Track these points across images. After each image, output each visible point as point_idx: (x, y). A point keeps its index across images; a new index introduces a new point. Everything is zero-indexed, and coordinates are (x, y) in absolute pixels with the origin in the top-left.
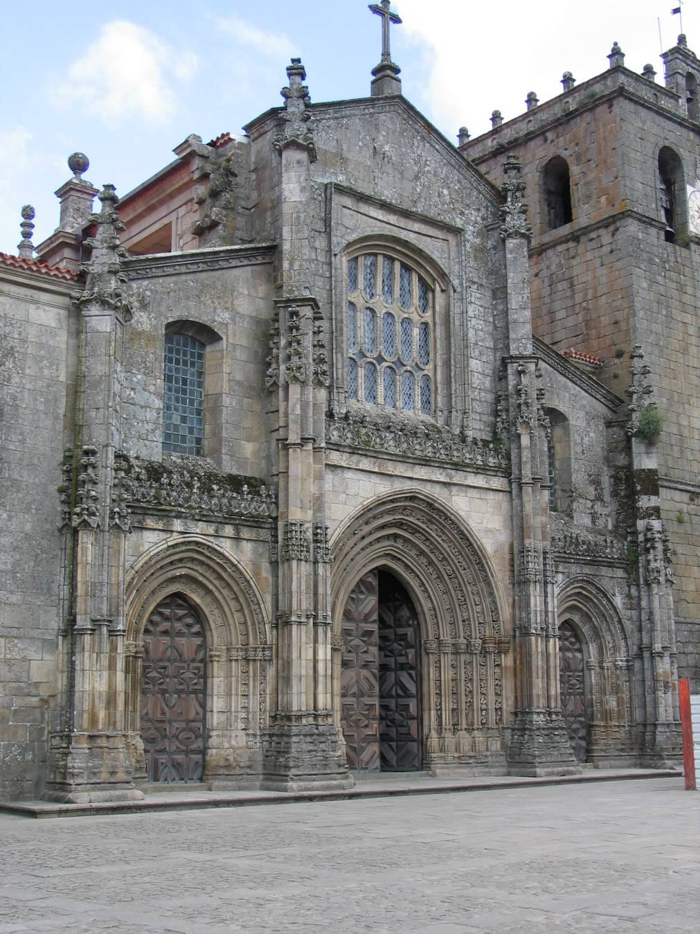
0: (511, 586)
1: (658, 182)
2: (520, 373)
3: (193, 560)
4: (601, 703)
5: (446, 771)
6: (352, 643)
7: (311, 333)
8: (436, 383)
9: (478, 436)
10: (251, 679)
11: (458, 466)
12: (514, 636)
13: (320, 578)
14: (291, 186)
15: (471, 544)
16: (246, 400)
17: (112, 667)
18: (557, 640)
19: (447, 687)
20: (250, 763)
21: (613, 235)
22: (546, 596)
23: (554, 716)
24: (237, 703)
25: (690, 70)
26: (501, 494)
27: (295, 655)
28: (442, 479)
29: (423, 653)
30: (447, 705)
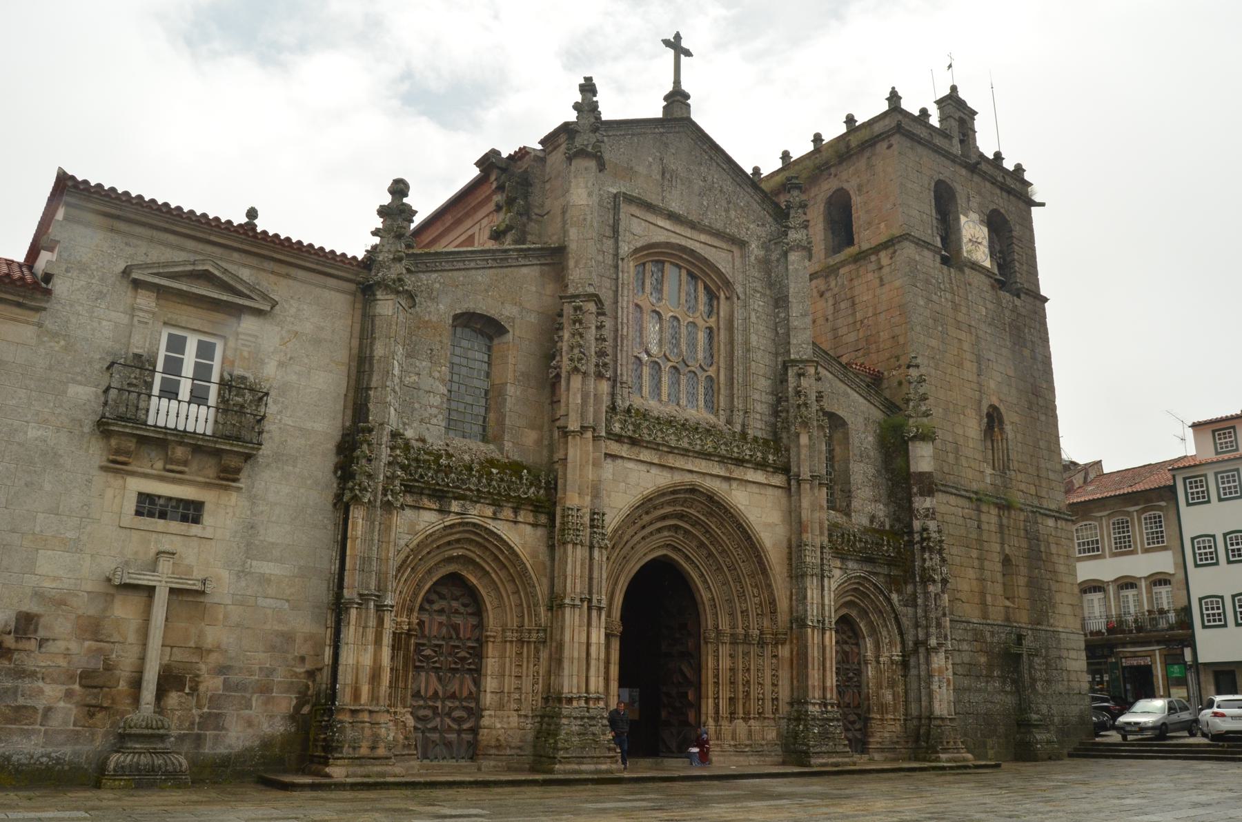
0: (788, 579)
1: (934, 211)
2: (800, 375)
3: (471, 541)
4: (878, 696)
5: (722, 759)
7: (594, 328)
8: (718, 383)
9: (759, 434)
10: (525, 660)
11: (740, 462)
12: (791, 628)
13: (595, 562)
14: (580, 191)
15: (749, 537)
16: (530, 390)
17: (378, 641)
18: (833, 633)
19: (724, 676)
20: (521, 744)
21: (891, 258)
22: (823, 590)
23: (829, 708)
24: (510, 683)
25: (963, 115)
26: (780, 490)
27: (567, 637)
28: (722, 473)
29: (702, 642)
30: (725, 694)
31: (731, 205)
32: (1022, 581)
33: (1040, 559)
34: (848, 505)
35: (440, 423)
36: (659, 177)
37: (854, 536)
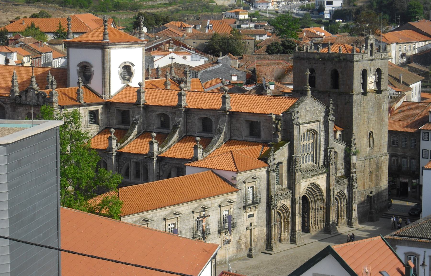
30: (314, 220)
32: (373, 176)
33: (379, 169)
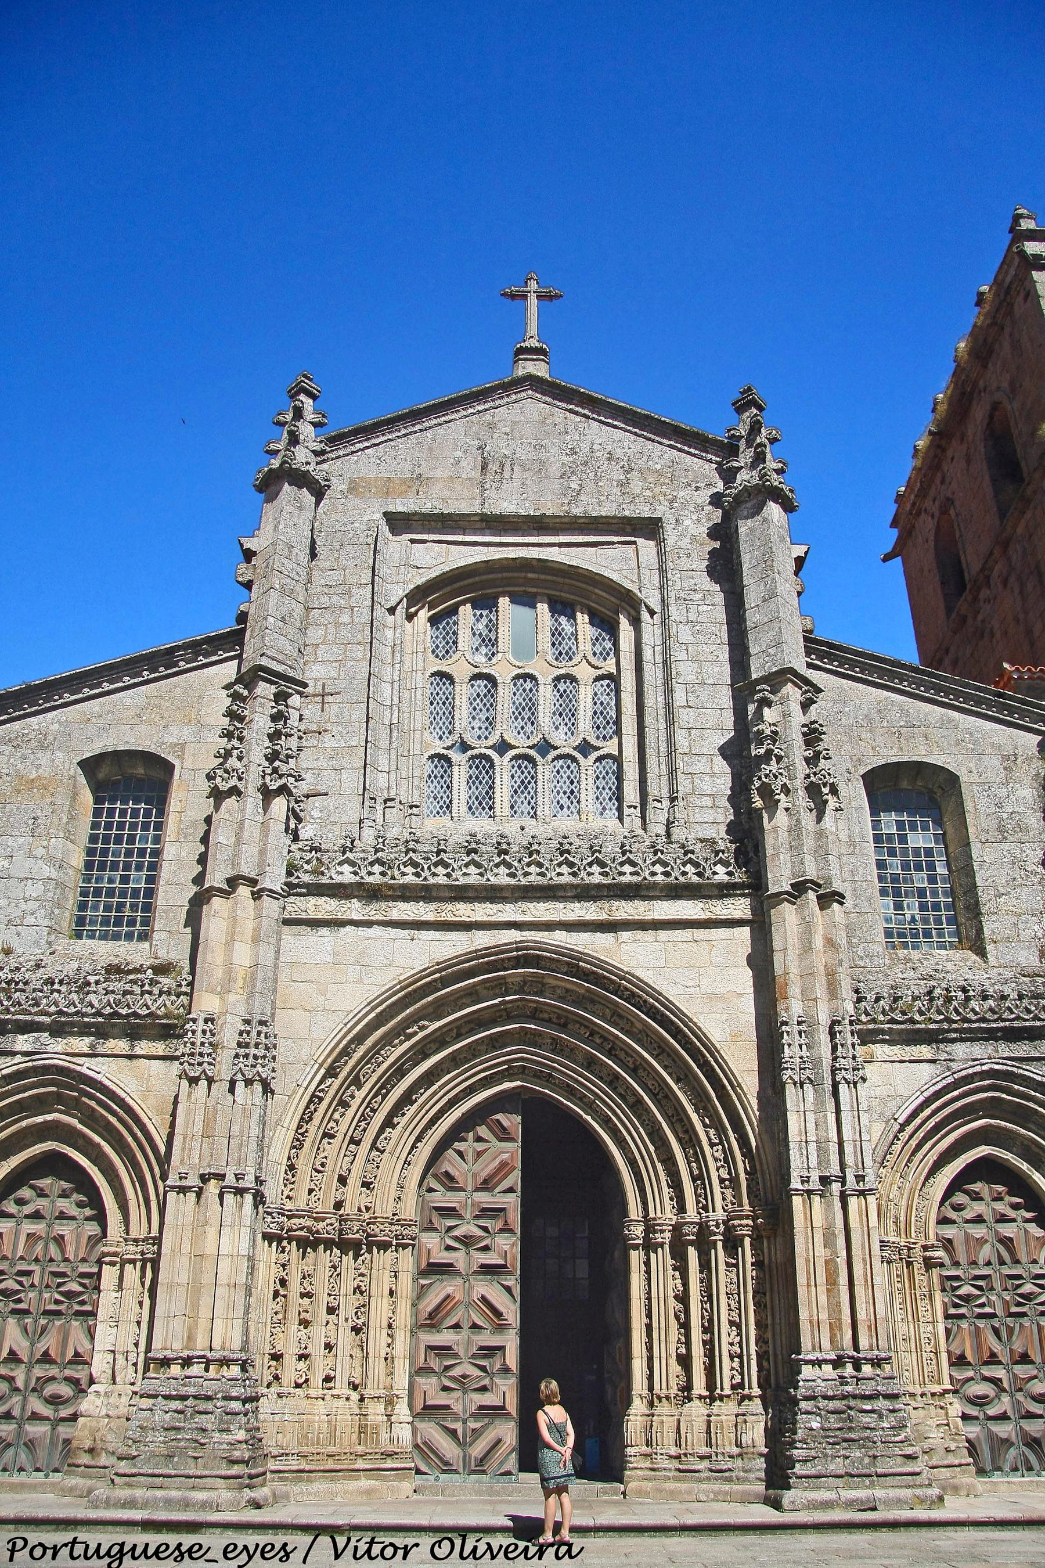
6: (456, 1233)
23: (867, 1369)
31: (634, 475)
34: (980, 931)
35: (40, 922)
36: (476, 474)
37: (964, 990)
